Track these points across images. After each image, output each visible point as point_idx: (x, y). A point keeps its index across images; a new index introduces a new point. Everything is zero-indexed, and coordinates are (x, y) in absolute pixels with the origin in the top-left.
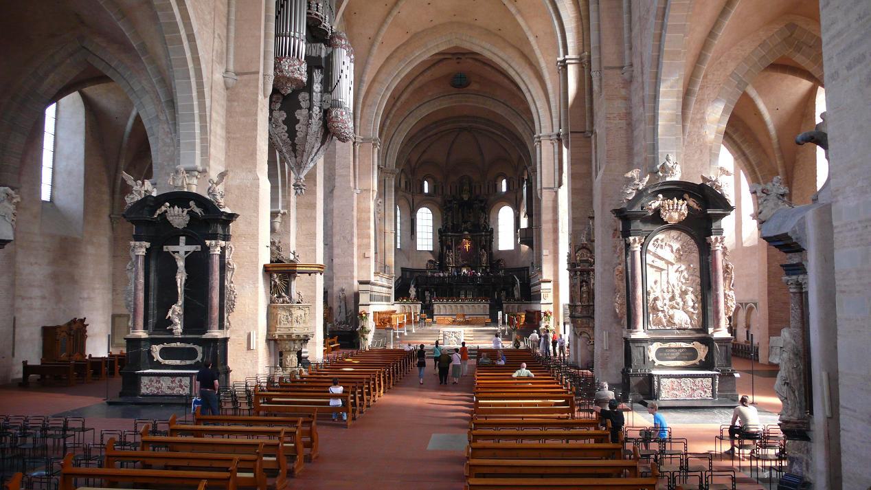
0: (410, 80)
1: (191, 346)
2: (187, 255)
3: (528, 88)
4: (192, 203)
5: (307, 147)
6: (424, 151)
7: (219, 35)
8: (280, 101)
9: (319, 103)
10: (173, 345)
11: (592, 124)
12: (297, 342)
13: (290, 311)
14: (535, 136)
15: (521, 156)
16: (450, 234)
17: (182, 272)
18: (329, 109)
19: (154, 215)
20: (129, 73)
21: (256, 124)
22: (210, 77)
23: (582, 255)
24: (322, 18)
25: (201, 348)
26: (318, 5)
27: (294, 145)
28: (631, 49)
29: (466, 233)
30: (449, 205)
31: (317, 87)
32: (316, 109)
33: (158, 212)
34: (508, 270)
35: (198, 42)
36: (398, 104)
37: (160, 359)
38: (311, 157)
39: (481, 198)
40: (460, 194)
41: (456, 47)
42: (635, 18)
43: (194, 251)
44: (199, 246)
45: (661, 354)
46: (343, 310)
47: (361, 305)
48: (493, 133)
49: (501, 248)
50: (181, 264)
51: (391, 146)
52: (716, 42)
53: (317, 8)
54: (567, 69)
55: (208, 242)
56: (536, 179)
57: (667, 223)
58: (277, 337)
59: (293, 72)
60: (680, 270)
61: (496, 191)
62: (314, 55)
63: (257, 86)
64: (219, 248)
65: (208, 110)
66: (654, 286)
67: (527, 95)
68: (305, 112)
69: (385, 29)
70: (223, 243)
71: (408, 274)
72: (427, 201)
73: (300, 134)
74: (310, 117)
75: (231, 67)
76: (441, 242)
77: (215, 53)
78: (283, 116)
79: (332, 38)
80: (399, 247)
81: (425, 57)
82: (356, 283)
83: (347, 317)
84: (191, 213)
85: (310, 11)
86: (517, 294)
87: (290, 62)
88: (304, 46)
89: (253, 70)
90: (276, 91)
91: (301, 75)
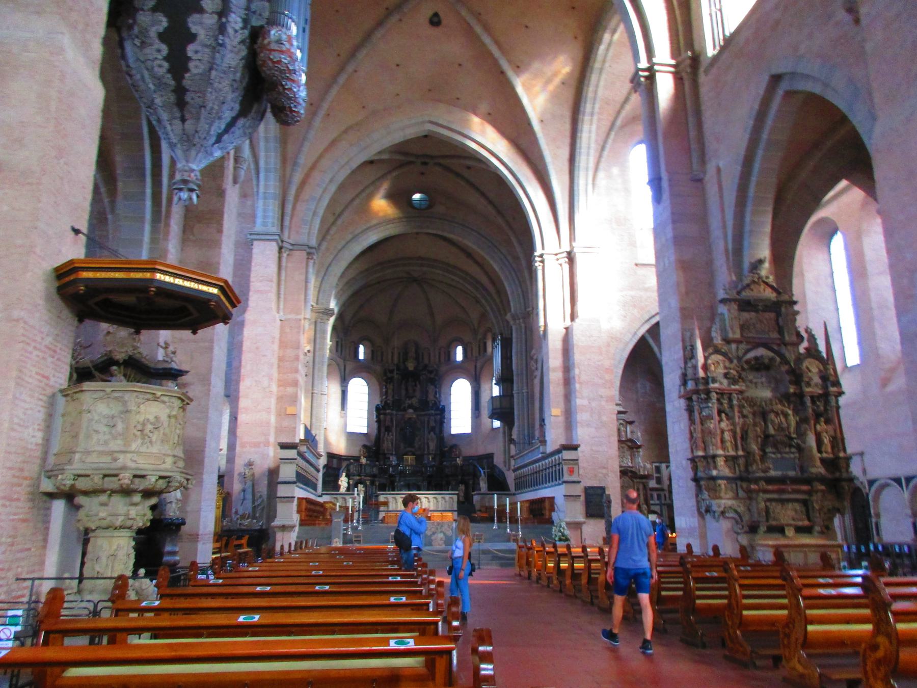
12: (137, 498)
13: (125, 403)
18: (262, 27)
27: (180, 92)
29: (411, 411)
30: (389, 375)
32: (235, 20)
34: (467, 459)
36: (339, 222)
39: (431, 369)
40: (404, 362)
46: (249, 496)
49: (454, 431)
68: (210, 20)
69: (334, 91)
71: (335, 461)
72: (361, 370)
73: (197, 67)
78: (163, 22)
83: (254, 508)
86: (483, 485)
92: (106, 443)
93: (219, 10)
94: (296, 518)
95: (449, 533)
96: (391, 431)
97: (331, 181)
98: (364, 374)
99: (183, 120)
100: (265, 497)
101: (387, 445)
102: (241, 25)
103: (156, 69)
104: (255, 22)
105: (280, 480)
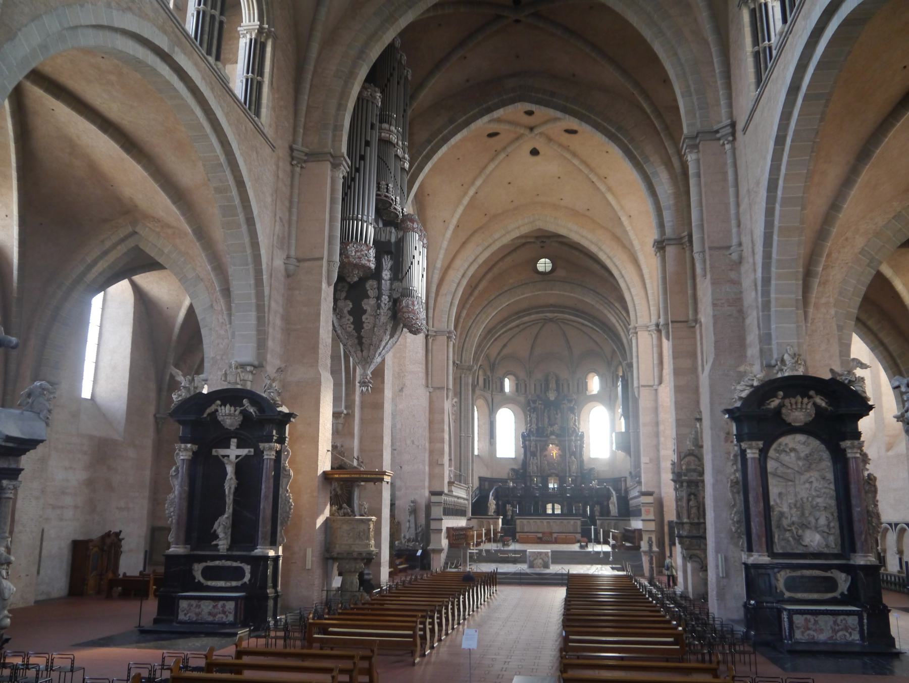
0: (490, 266)
1: (235, 564)
2: (237, 460)
3: (621, 273)
4: (245, 401)
5: (375, 339)
6: (505, 346)
7: (280, 218)
8: (346, 289)
10: (217, 563)
11: (696, 311)
14: (630, 327)
15: (614, 351)
16: (534, 438)
17: (232, 478)
18: (399, 298)
19: (203, 415)
20: (182, 260)
21: (319, 315)
22: (270, 264)
23: (688, 464)
24: (392, 200)
25: (249, 567)
26: (388, 185)
27: (360, 339)
28: (739, 225)
29: (553, 437)
31: (386, 275)
32: (385, 299)
33: (208, 411)
34: (600, 482)
35: (258, 226)
36: (476, 293)
37: (202, 580)
38: (379, 351)
40: (545, 393)
41: (540, 230)
42: (743, 191)
43: (246, 456)
44: (252, 450)
45: (791, 585)
46: (413, 525)
47: (433, 519)
48: (583, 324)
49: (593, 455)
50: (230, 469)
51: (467, 339)
52: (841, 216)
53: (387, 189)
54: (665, 252)
55: (262, 445)
56: (632, 375)
57: (790, 424)
58: (335, 556)
59: (360, 258)
60: (811, 480)
61: (586, 389)
62: (383, 239)
63: (321, 274)
64: (274, 453)
65: (266, 299)
66: (778, 501)
67: (621, 281)
68: (372, 302)
70: (278, 446)
71: (487, 484)
72: (507, 401)
73: (367, 326)
74: (379, 307)
75: (293, 253)
76: (525, 447)
77: (276, 237)
79: (403, 221)
80: (476, 453)
81: (506, 240)
82: (427, 493)
83: (417, 534)
84: (244, 413)
85: (379, 193)
87: (357, 247)
88: (373, 230)
89: (317, 256)
90: (341, 278)
91: (369, 261)
92: (347, 540)
93: (377, 295)
94: (445, 543)
95: (546, 559)
96: (536, 456)
97: (463, 276)
98: (511, 405)
99: (362, 351)
100: (424, 526)
101: (532, 468)
102: (388, 300)
103: (348, 329)
104: (395, 296)
105: (432, 517)
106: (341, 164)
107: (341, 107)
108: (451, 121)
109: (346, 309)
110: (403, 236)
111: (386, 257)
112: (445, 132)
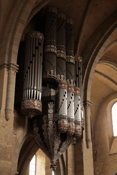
8: (36, 122)
9: (53, 119)
18: (57, 121)
26: (50, 71)
27: (45, 144)
31: (51, 111)
32: (51, 122)
59: (29, 106)
62: (48, 96)
73: (46, 137)
74: (48, 126)
87: (28, 101)
91: (35, 106)
99: (48, 150)
102: (52, 123)
104: (56, 120)
106: (10, 67)
107: (12, 44)
108: (102, 35)
109: (37, 131)
110: (58, 92)
111: (50, 103)
112: (100, 41)
